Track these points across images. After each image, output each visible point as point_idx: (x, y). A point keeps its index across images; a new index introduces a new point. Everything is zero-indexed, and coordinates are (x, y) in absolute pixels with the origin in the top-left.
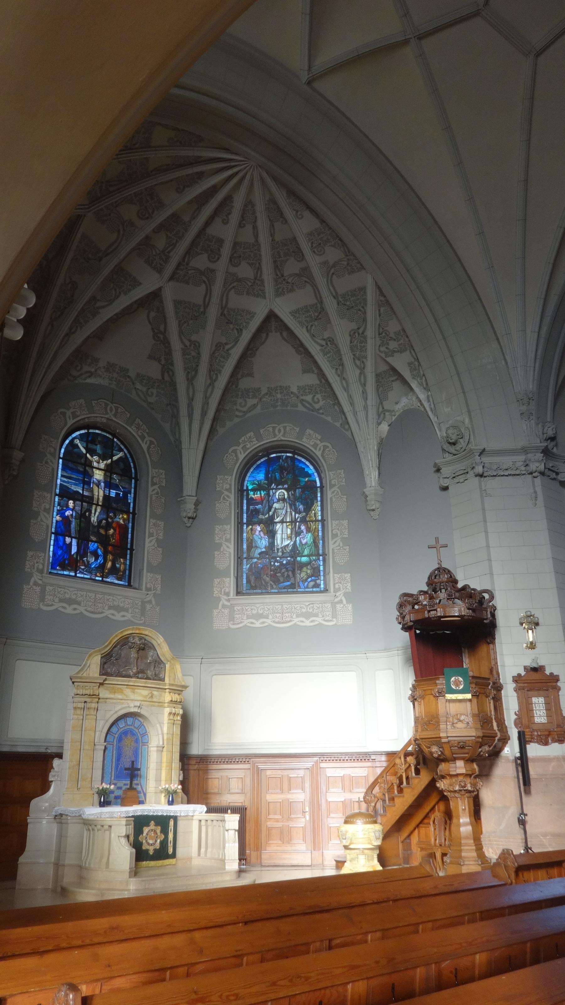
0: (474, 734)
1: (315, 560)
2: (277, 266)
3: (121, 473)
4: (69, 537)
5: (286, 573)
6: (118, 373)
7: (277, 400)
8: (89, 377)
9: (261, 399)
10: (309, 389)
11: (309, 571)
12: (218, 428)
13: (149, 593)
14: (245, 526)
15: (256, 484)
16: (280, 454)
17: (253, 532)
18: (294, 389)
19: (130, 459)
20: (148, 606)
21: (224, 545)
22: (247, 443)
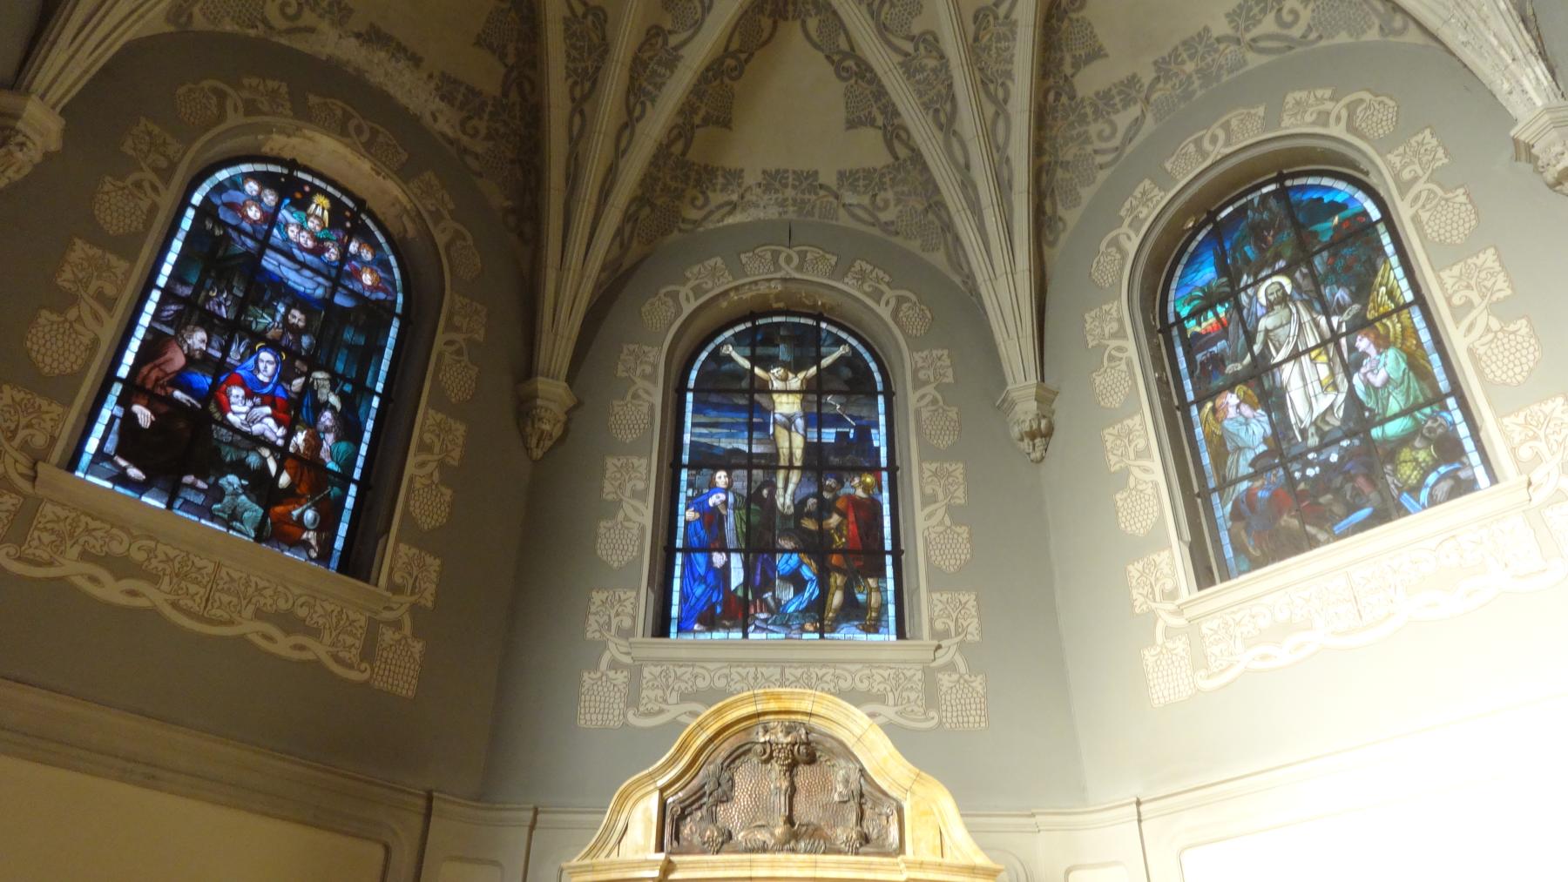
1: (1433, 418)
3: (845, 388)
4: (720, 551)
5: (1348, 487)
6: (794, 187)
7: (1189, 77)
8: (730, 213)
9: (1147, 99)
12: (1061, 211)
13: (944, 643)
14: (1194, 410)
15: (1199, 297)
16: (1244, 201)
18: (1221, 28)
19: (867, 356)
20: (946, 680)
21: (1136, 472)
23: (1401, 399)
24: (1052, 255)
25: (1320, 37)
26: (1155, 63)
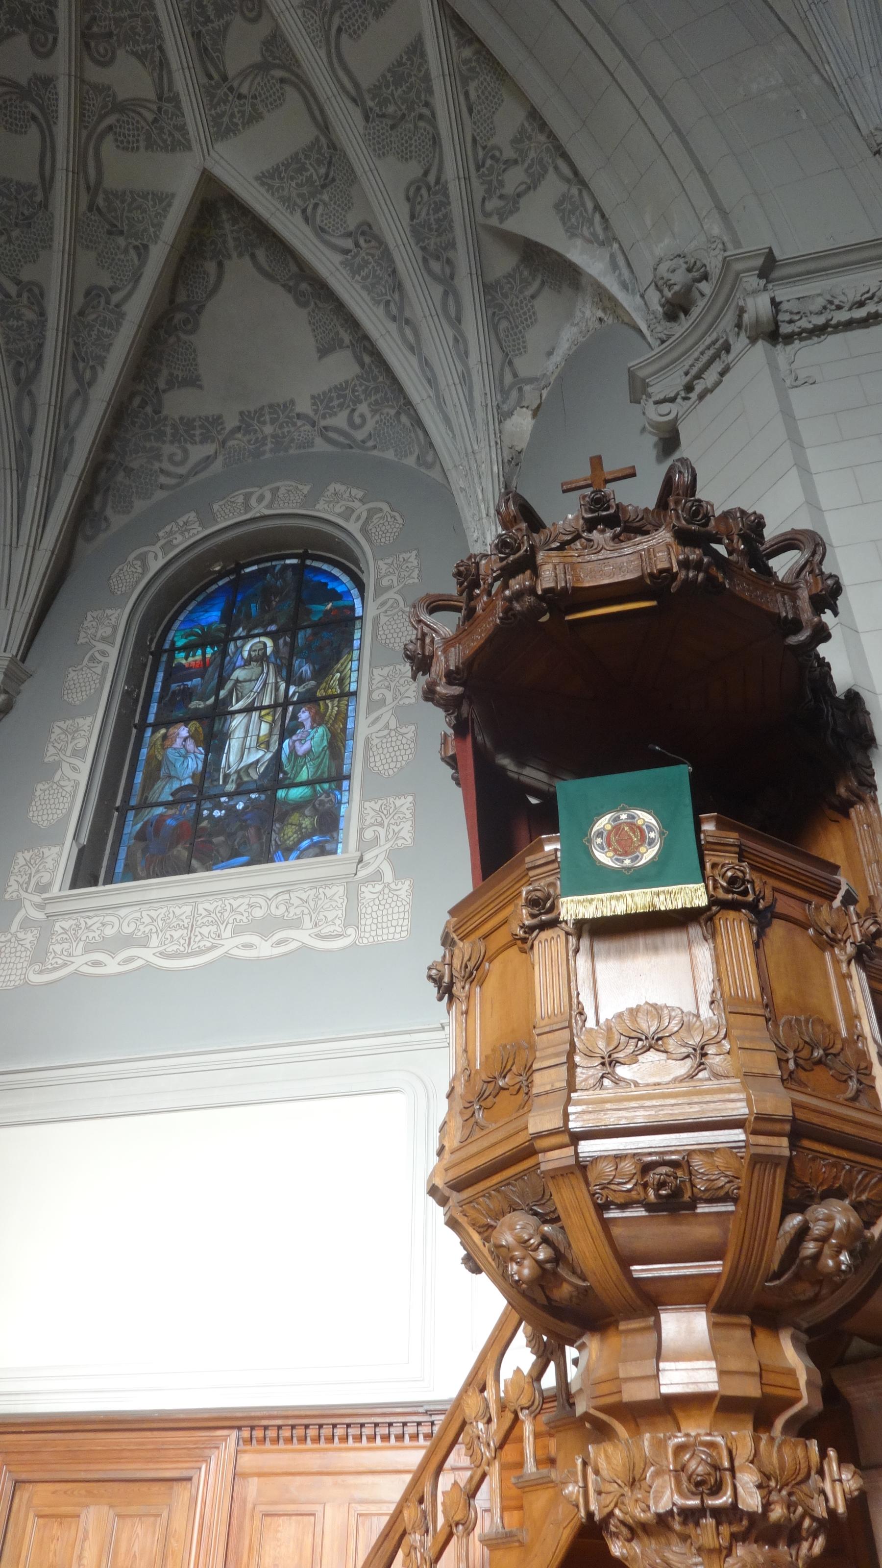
0: (740, 1109)
2: (206, 49)
5: (240, 834)
7: (265, 438)
9: (224, 443)
10: (338, 398)
11: (306, 823)
12: (109, 512)
14: (149, 732)
15: (196, 634)
16: (269, 564)
17: (167, 743)
18: (304, 406)
21: (65, 767)
22: (177, 535)
23: (311, 770)
24: (85, 549)
25: (375, 447)
26: (241, 413)
